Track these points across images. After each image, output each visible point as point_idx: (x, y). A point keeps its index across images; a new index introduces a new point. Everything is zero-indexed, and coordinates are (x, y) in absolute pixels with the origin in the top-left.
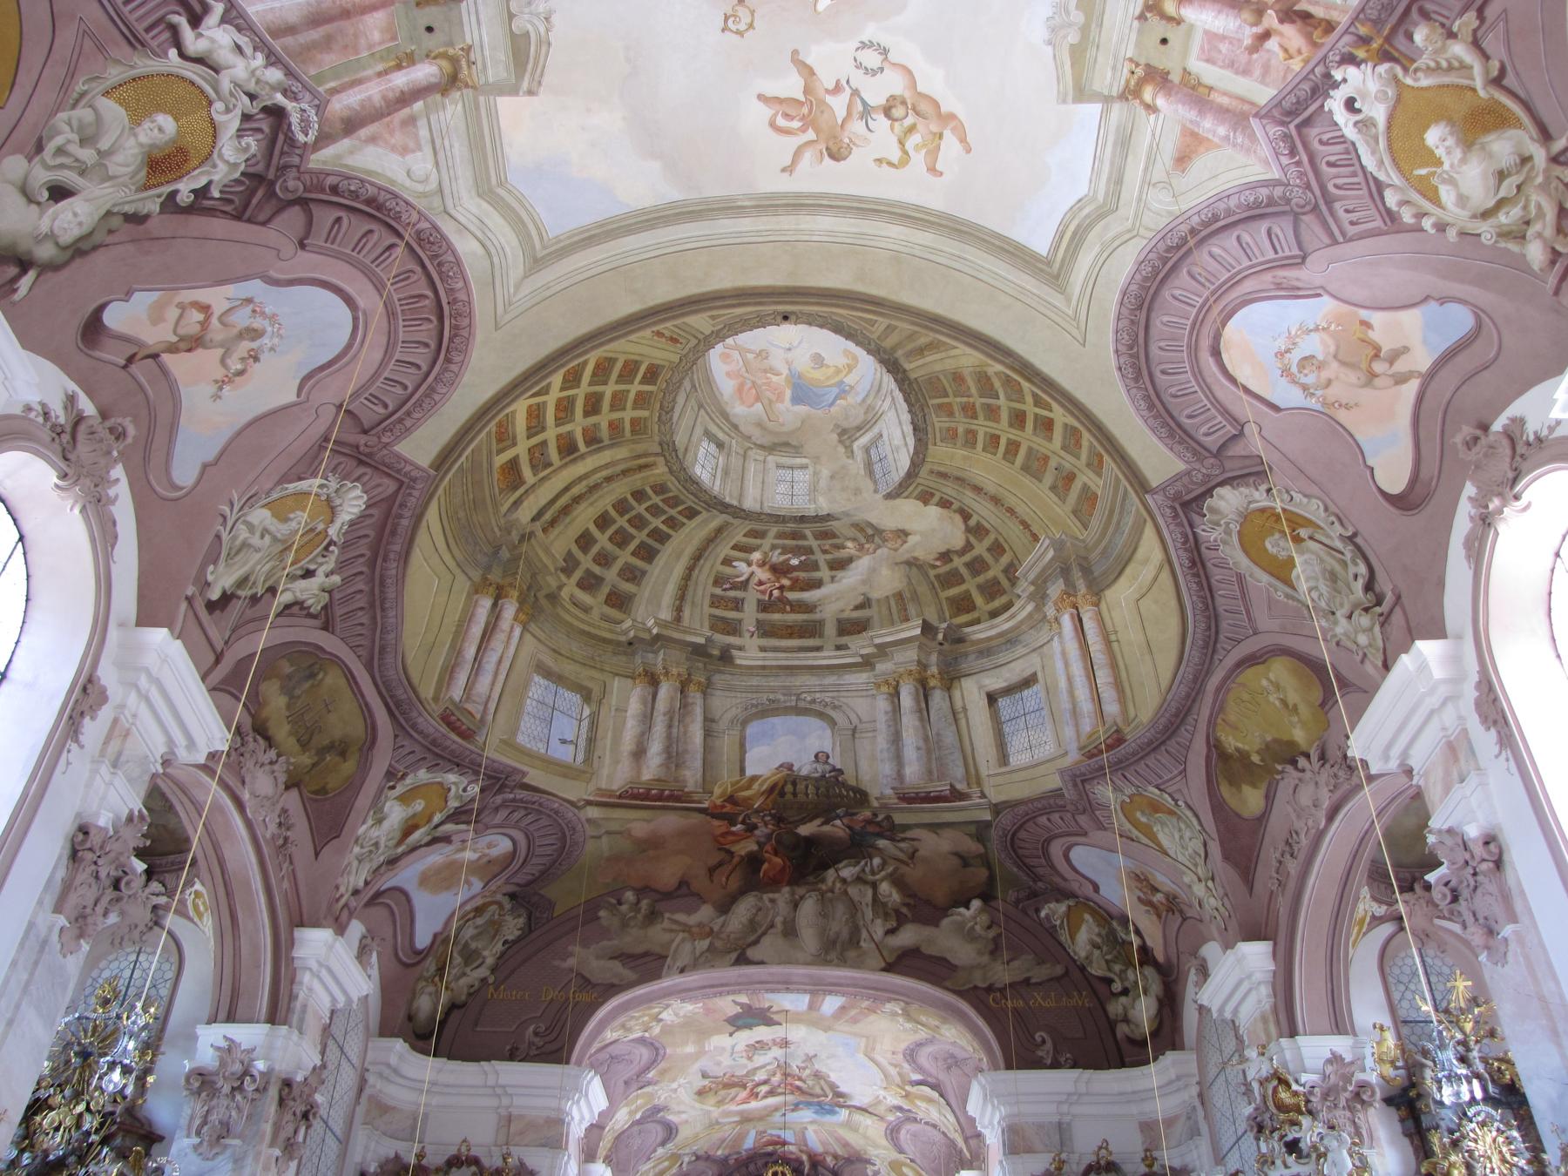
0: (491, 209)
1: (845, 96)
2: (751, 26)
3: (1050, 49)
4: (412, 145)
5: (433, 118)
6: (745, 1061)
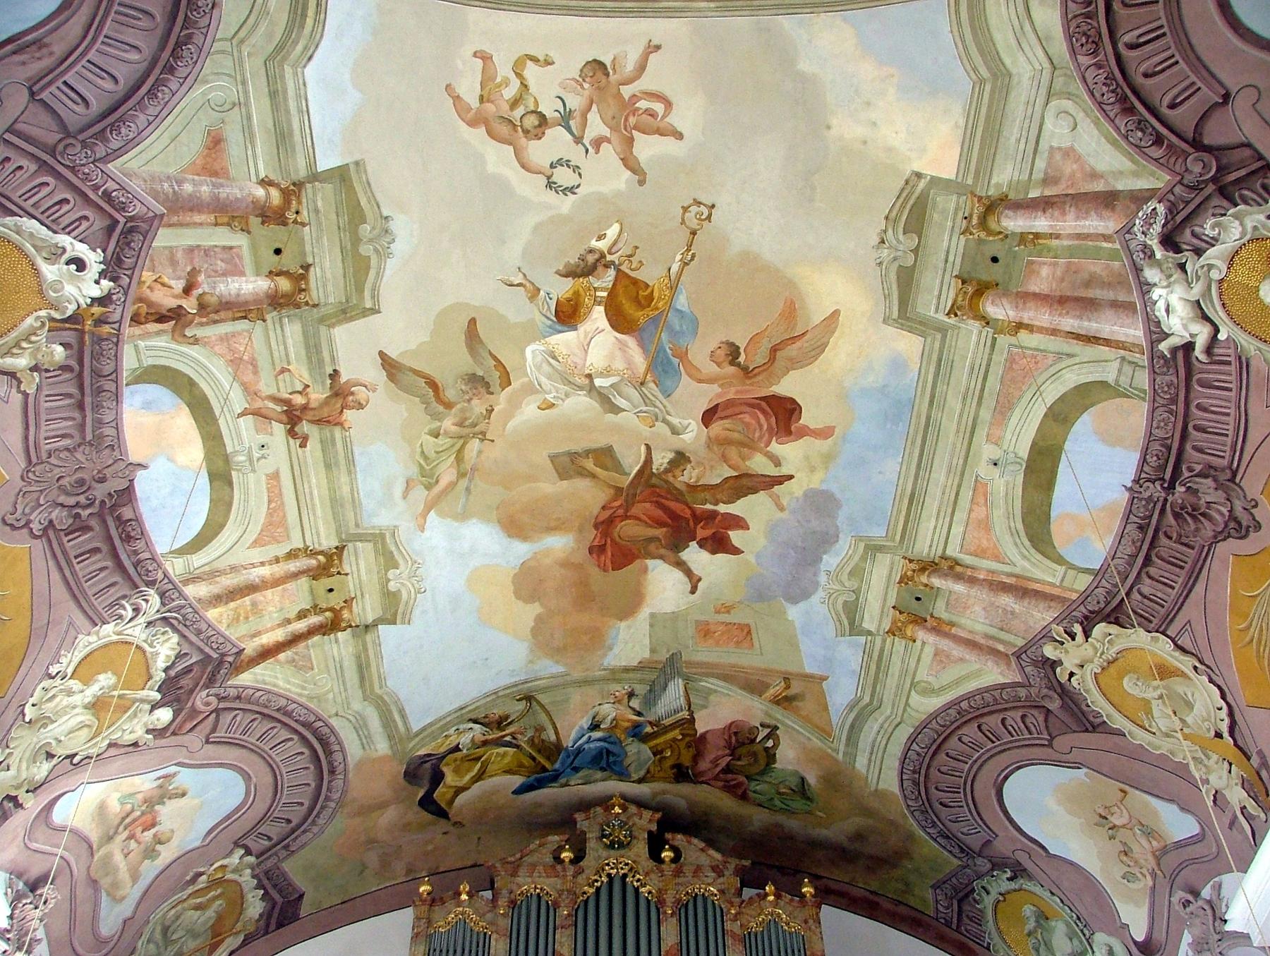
0: (1003, 55)
1: (589, 136)
2: (685, 209)
3: (385, 213)
4: (1058, 157)
5: (1025, 177)
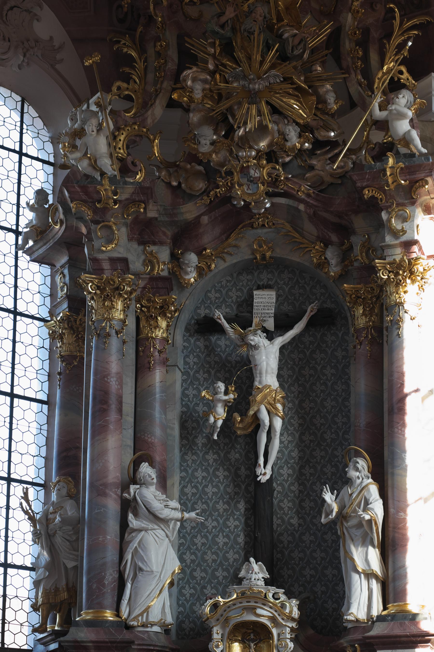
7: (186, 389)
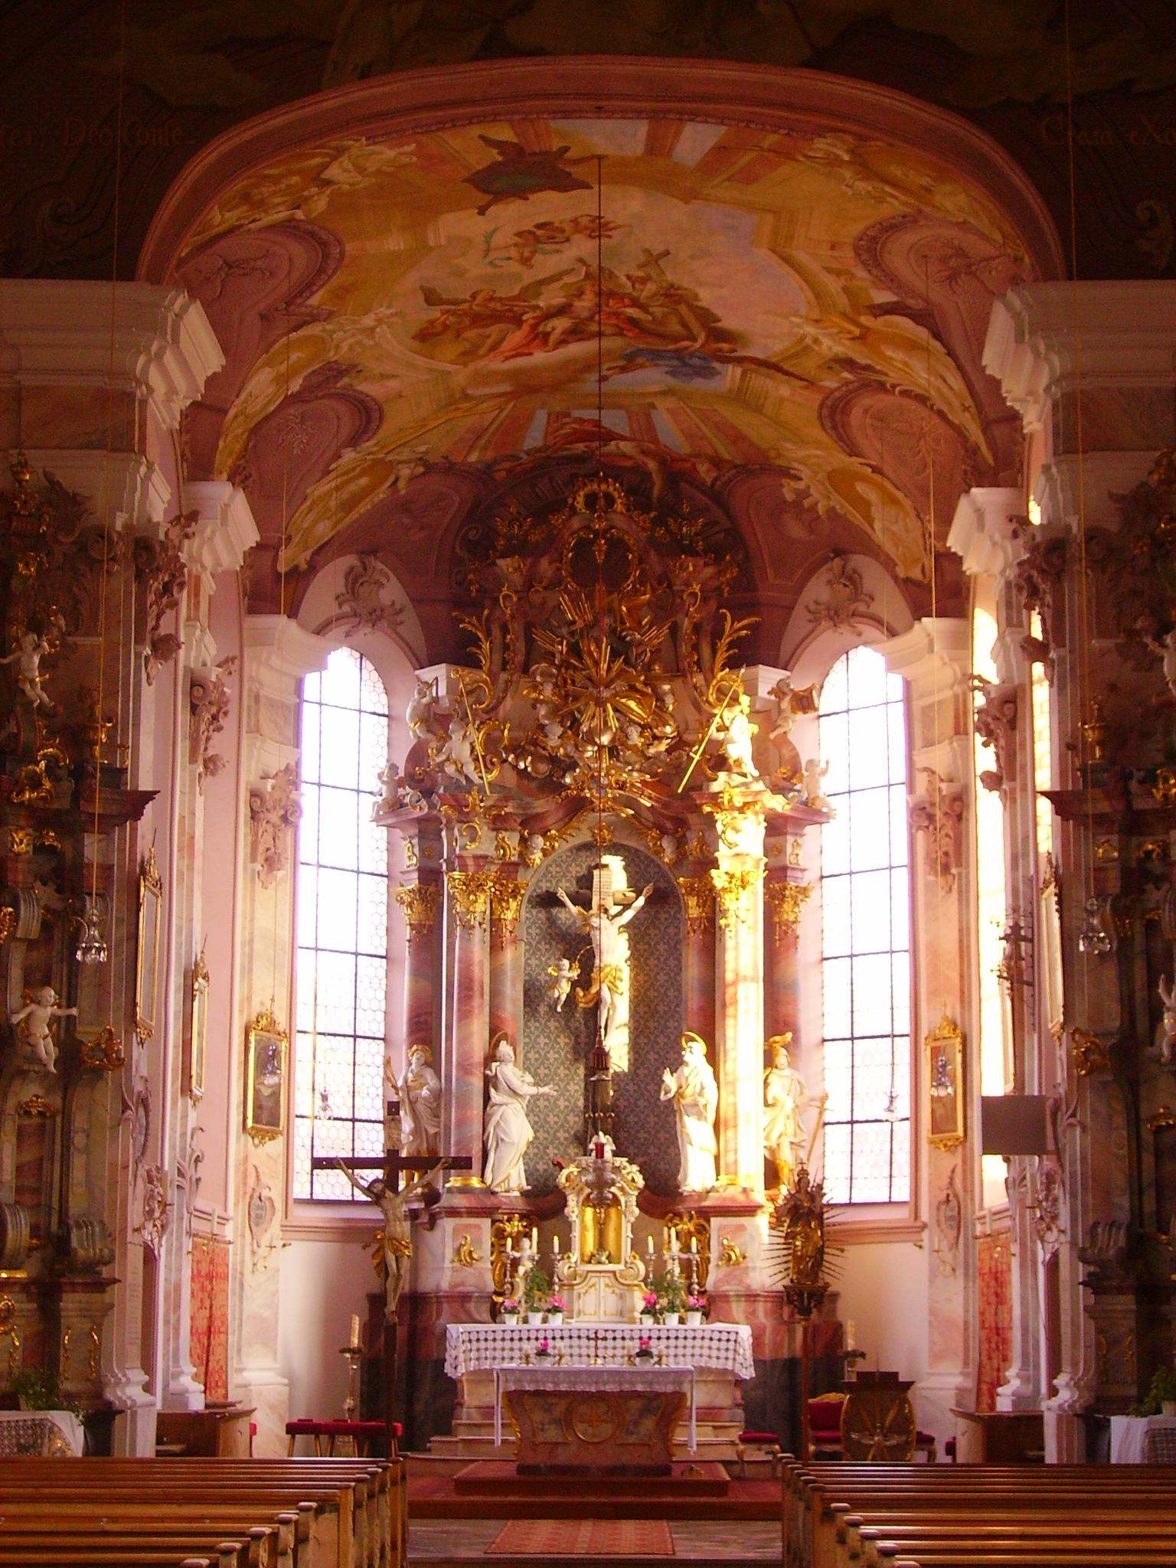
6: (515, 267)
7: (530, 959)
